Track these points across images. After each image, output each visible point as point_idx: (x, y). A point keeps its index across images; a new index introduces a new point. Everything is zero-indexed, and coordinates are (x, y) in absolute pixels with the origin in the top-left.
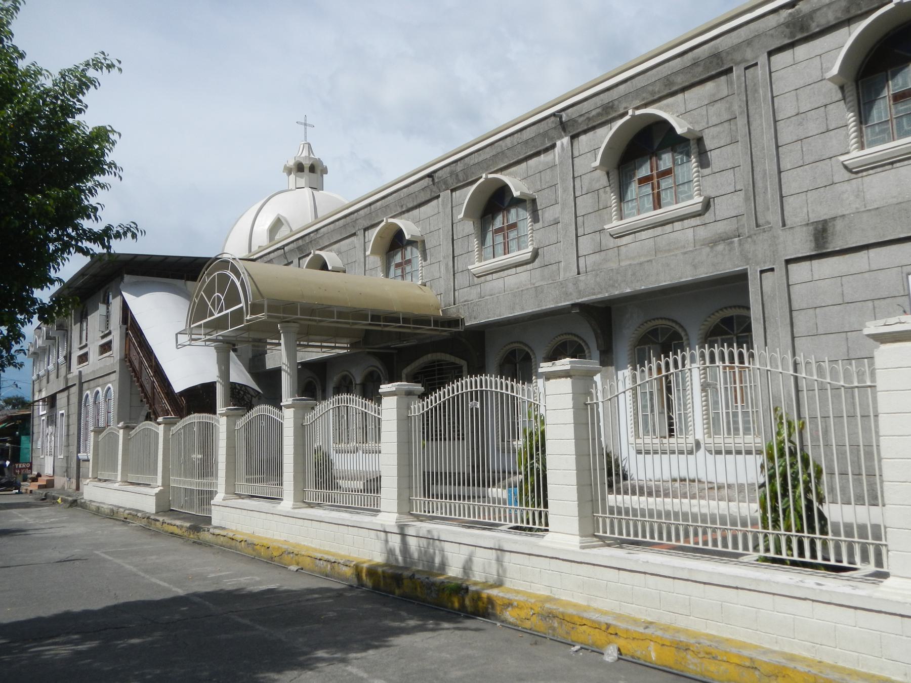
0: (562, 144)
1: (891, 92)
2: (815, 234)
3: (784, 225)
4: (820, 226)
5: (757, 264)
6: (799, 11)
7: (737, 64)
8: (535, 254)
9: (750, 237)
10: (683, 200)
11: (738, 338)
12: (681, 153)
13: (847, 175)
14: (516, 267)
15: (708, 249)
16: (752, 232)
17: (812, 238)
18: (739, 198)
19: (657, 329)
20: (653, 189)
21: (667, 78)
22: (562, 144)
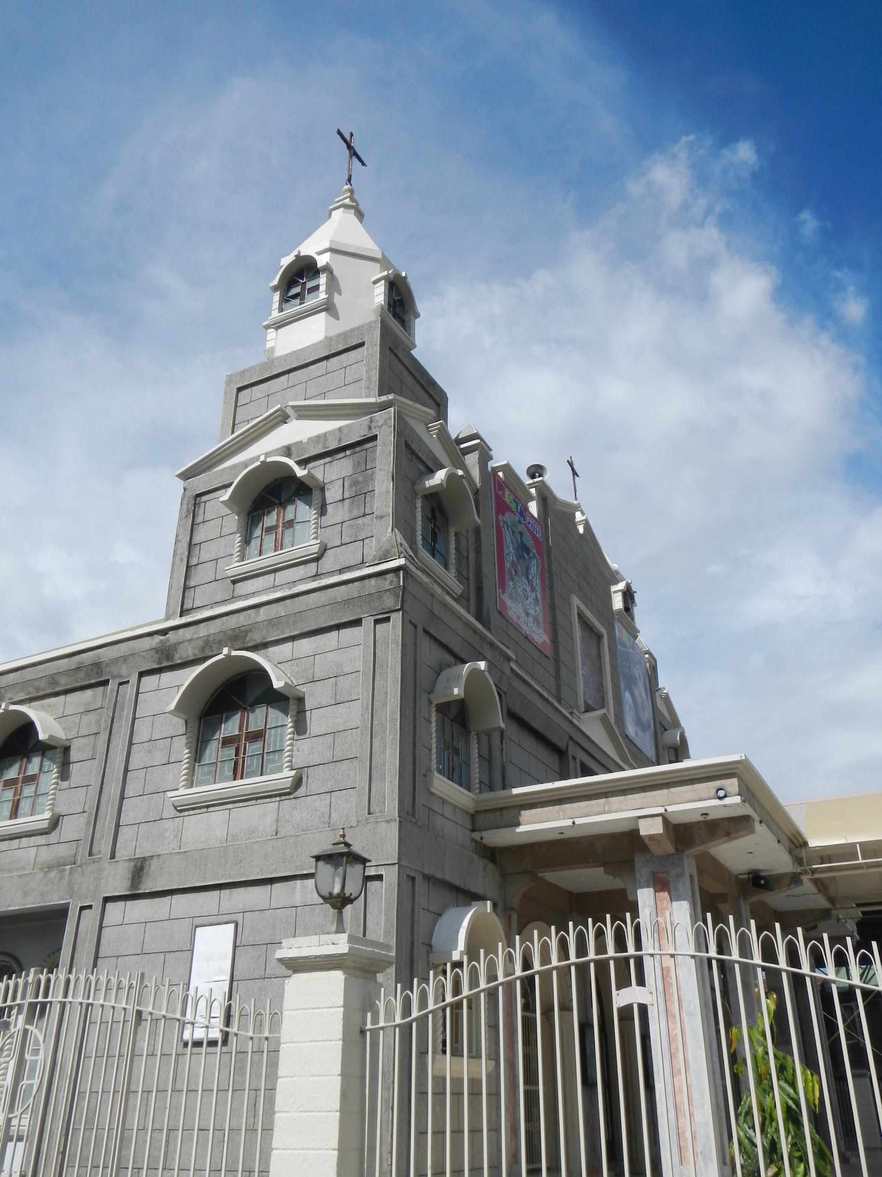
1: (222, 736)
2: (133, 872)
3: (113, 856)
4: (139, 864)
6: (168, 640)
7: (114, 677)
9: (80, 866)
10: (39, 814)
12: (50, 759)
13: (174, 813)
15: (42, 875)
16: (84, 861)
17: (130, 876)
18: (82, 820)
20: (15, 795)
21: (53, 676)
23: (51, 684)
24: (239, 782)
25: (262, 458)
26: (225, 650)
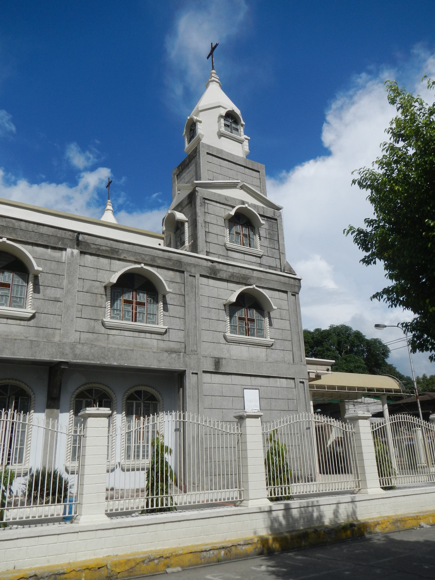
0: (72, 253)
2: (215, 363)
4: (217, 360)
5: (191, 369)
6: (215, 267)
7: (187, 271)
8: (33, 317)
11: (144, 403)
12: (151, 297)
13: (225, 342)
14: (7, 318)
17: (214, 364)
19: (92, 389)
20: (133, 310)
21: (154, 257)
22: (72, 253)
23: (151, 260)
24: (247, 337)
25: (247, 205)
26: (254, 286)
